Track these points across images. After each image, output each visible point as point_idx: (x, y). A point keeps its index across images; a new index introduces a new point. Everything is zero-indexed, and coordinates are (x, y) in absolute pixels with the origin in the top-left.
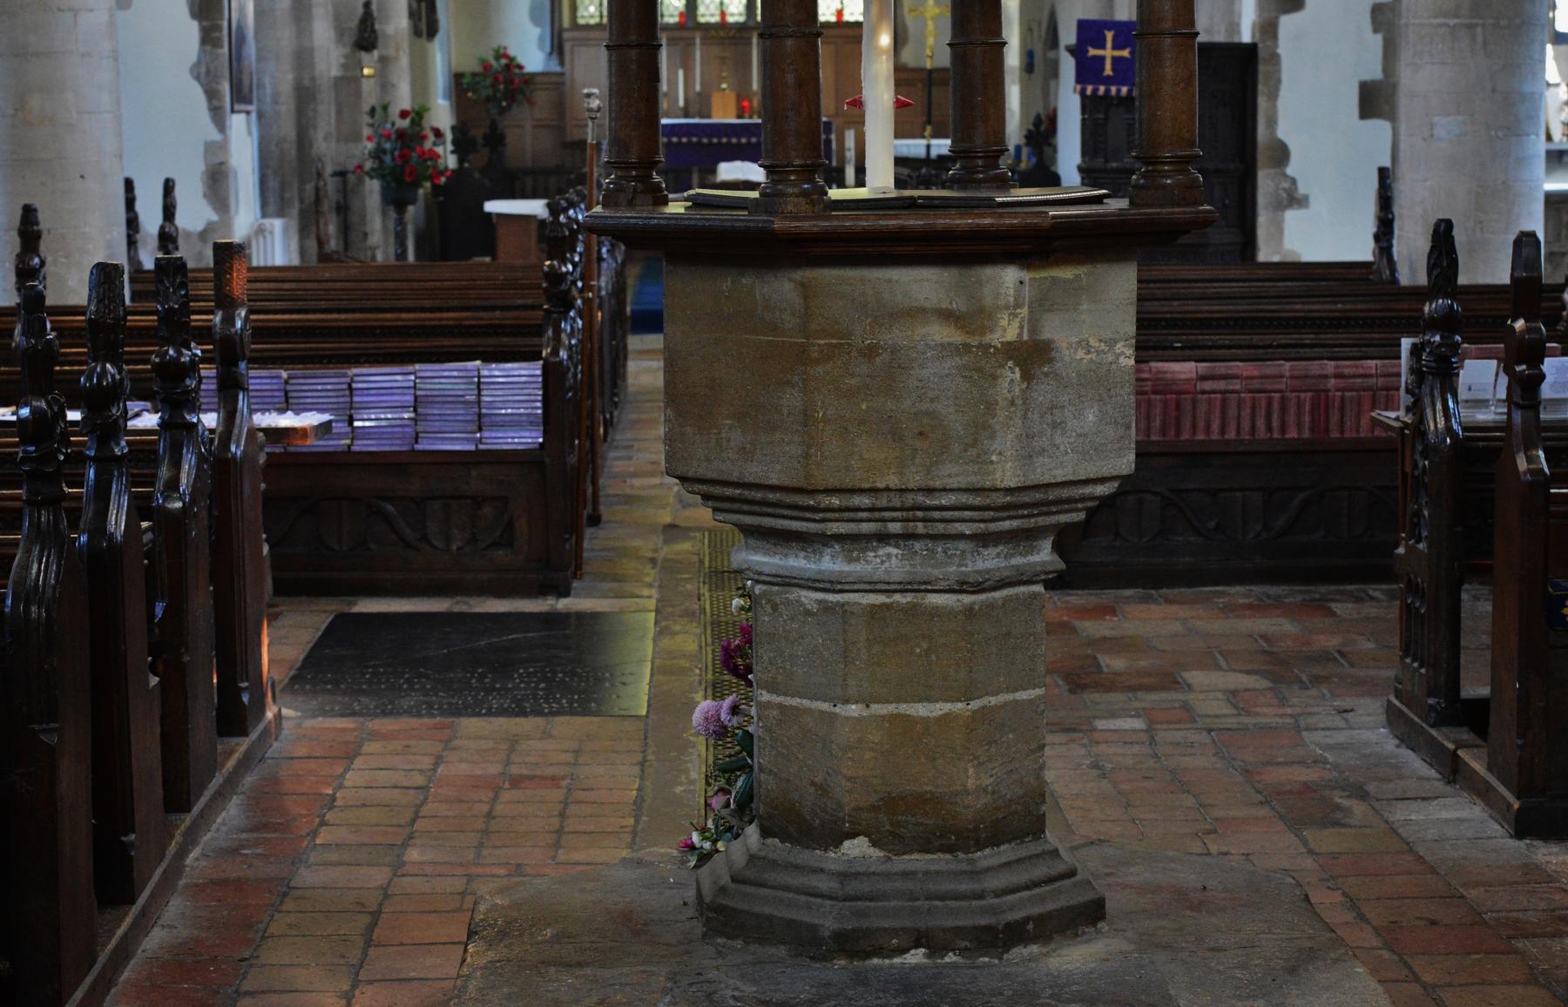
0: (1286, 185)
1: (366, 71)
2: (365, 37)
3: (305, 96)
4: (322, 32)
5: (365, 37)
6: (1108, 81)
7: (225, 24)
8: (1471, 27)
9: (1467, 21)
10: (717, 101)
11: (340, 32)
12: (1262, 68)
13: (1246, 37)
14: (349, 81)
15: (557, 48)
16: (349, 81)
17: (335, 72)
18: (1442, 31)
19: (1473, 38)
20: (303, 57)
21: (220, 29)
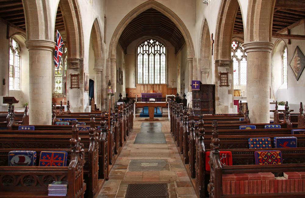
0: (219, 102)
1: (110, 88)
2: (109, 84)
3: (102, 90)
4: (105, 84)
5: (109, 84)
6: (196, 88)
7: (84, 81)
8: (259, 81)
9: (258, 80)
10: (151, 91)
11: (107, 83)
12: (216, 88)
13: (213, 83)
14: (108, 88)
15: (136, 86)
16: (108, 88)
17: (106, 88)
18: (254, 81)
19: (260, 83)
20: (102, 86)
21: (83, 82)
